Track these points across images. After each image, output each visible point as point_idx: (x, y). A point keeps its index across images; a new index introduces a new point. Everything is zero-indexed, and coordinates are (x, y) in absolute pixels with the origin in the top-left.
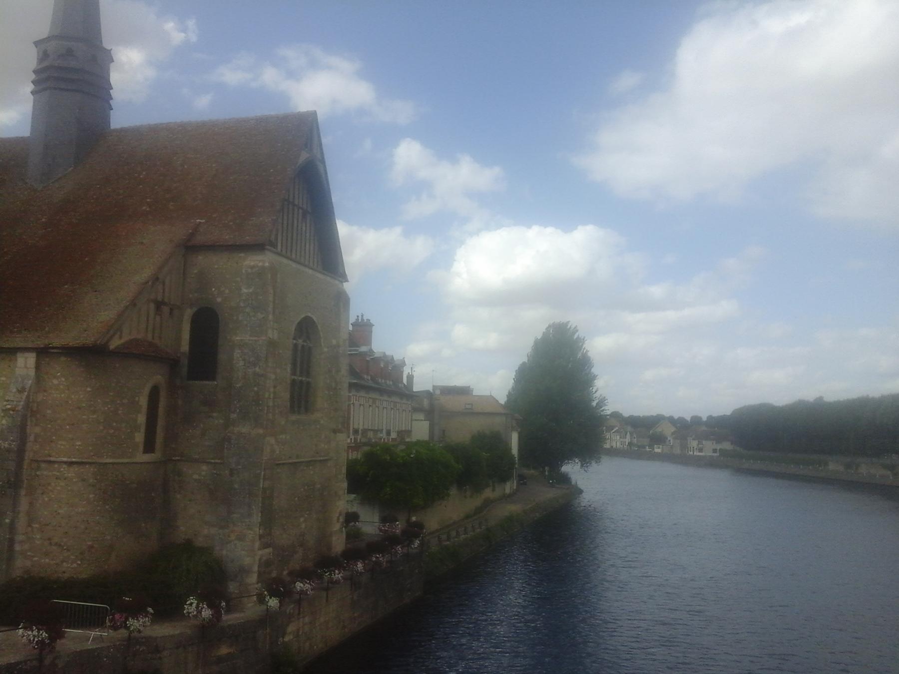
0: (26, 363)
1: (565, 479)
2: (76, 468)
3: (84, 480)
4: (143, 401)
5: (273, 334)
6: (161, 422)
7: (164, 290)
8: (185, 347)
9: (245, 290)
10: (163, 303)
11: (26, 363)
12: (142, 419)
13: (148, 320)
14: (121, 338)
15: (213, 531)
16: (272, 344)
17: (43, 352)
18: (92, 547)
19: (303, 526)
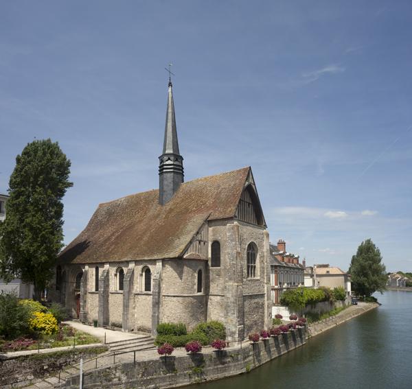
0: (159, 264)
1: (375, 300)
5: (239, 249)
8: (210, 256)
9: (228, 234)
11: (159, 264)
12: (196, 281)
15: (223, 319)
16: (238, 253)
17: (164, 261)
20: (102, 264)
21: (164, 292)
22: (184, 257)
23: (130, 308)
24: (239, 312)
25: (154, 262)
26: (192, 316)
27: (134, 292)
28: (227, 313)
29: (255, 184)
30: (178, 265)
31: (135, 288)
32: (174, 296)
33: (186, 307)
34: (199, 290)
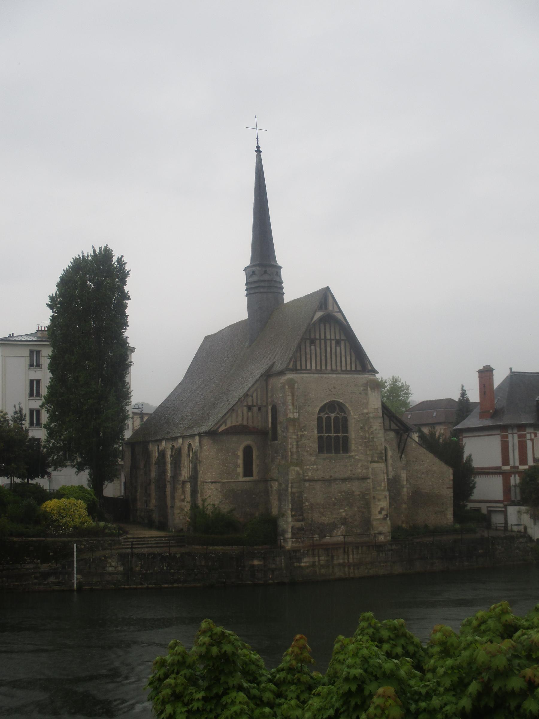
2: (214, 484)
3: (217, 489)
4: (240, 453)
7: (253, 400)
8: (270, 425)
10: (253, 406)
12: (240, 461)
13: (243, 416)
14: (226, 426)
19: (344, 514)
20: (160, 441)
21: (201, 477)
22: (220, 430)
23: (176, 501)
25: (193, 436)
27: (182, 478)
29: (340, 311)
31: (183, 473)
32: (212, 483)
34: (248, 472)
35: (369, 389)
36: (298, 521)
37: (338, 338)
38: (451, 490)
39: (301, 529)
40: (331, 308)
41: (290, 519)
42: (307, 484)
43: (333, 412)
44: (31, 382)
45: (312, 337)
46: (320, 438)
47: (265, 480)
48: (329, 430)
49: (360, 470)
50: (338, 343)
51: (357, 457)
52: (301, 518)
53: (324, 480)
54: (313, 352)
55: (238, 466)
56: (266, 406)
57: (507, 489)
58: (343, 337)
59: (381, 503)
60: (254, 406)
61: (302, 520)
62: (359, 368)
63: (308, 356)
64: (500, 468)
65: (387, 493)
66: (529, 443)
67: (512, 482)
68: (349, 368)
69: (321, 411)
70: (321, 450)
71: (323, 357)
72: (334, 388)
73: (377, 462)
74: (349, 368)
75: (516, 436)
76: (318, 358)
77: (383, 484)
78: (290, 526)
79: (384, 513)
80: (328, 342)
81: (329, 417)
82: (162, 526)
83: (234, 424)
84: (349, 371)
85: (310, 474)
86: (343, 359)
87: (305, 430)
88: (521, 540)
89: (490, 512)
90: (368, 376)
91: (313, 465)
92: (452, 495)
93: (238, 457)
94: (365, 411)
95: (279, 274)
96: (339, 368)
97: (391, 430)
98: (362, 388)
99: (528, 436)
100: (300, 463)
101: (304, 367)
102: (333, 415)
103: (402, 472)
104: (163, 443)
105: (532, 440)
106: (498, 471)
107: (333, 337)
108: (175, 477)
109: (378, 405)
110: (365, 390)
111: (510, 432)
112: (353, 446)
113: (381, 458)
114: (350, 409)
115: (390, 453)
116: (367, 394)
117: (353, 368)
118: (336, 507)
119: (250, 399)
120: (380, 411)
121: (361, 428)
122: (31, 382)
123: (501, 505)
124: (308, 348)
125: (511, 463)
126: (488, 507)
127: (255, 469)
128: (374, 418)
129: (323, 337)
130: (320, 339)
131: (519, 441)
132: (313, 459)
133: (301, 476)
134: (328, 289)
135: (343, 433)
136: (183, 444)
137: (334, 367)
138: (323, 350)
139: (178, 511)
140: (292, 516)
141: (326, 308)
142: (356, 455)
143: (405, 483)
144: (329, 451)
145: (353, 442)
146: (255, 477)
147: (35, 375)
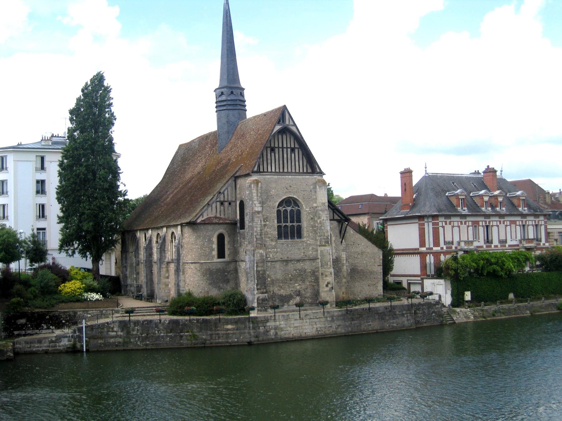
2: (193, 264)
4: (215, 240)
6: (227, 247)
8: (238, 217)
12: (215, 246)
17: (182, 225)
18: (201, 292)
22: (199, 221)
24: (259, 278)
26: (210, 284)
27: (167, 260)
28: (248, 280)
29: (295, 125)
30: (194, 230)
31: (167, 255)
33: (204, 274)
34: (221, 254)
35: (318, 187)
36: (262, 293)
37: (293, 146)
38: (382, 267)
39: (263, 300)
40: (287, 123)
41: (256, 292)
42: (269, 264)
43: (289, 206)
44: (38, 182)
45: (273, 145)
46: (279, 227)
47: (235, 261)
48: (286, 221)
49: (311, 252)
50: (293, 150)
51: (308, 242)
52: (265, 290)
53: (283, 261)
54: (273, 158)
55: (213, 250)
56: (235, 202)
57: (424, 266)
58: (297, 146)
59: (328, 278)
60: (226, 201)
61: (266, 293)
62: (309, 171)
63: (269, 161)
64: (418, 249)
65: (332, 270)
66: (441, 230)
67: (428, 261)
68: (301, 171)
69: (280, 205)
70: (280, 236)
71: (281, 162)
72: (290, 186)
73: (325, 246)
74: (301, 171)
75: (431, 224)
76: (277, 163)
77: (329, 263)
78: (256, 297)
79: (330, 286)
80: (285, 150)
81: (286, 211)
82: (151, 297)
83: (210, 216)
84: (301, 173)
85: (271, 256)
86: (297, 163)
87: (267, 221)
88: (437, 306)
89: (409, 284)
90: (316, 177)
91: (274, 248)
92: (382, 271)
93: (213, 243)
94: (315, 205)
95: (242, 95)
96: (293, 171)
97: (333, 220)
98: (312, 187)
99: (440, 224)
100: (263, 245)
101: (265, 170)
102: (289, 209)
103: (343, 253)
104: (150, 232)
105: (443, 227)
106: (416, 251)
107: (289, 146)
108: (161, 259)
109: (325, 200)
110: (315, 188)
111: (426, 220)
112: (305, 233)
113: (327, 242)
114: (303, 203)
115: (333, 239)
116: (316, 192)
117: (305, 171)
118: (291, 282)
119: (222, 196)
120: (327, 204)
121: (312, 219)
122: (38, 182)
123: (419, 278)
124: (269, 155)
125: (427, 246)
126: (408, 280)
127: (227, 252)
128: (321, 210)
129: (281, 146)
130: (279, 148)
131: (433, 228)
132: (274, 243)
133: (265, 258)
134: (285, 106)
135: (297, 222)
136: (166, 232)
137: (290, 170)
138: (281, 156)
139: (164, 286)
140: (257, 289)
141: (283, 122)
142: (307, 240)
143: (345, 262)
144: (286, 237)
145: (305, 230)
146: (227, 259)
147: (41, 176)
